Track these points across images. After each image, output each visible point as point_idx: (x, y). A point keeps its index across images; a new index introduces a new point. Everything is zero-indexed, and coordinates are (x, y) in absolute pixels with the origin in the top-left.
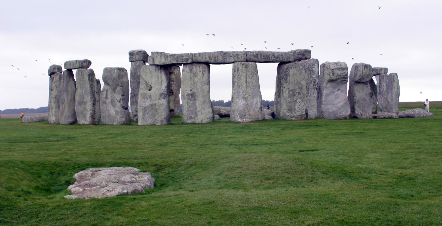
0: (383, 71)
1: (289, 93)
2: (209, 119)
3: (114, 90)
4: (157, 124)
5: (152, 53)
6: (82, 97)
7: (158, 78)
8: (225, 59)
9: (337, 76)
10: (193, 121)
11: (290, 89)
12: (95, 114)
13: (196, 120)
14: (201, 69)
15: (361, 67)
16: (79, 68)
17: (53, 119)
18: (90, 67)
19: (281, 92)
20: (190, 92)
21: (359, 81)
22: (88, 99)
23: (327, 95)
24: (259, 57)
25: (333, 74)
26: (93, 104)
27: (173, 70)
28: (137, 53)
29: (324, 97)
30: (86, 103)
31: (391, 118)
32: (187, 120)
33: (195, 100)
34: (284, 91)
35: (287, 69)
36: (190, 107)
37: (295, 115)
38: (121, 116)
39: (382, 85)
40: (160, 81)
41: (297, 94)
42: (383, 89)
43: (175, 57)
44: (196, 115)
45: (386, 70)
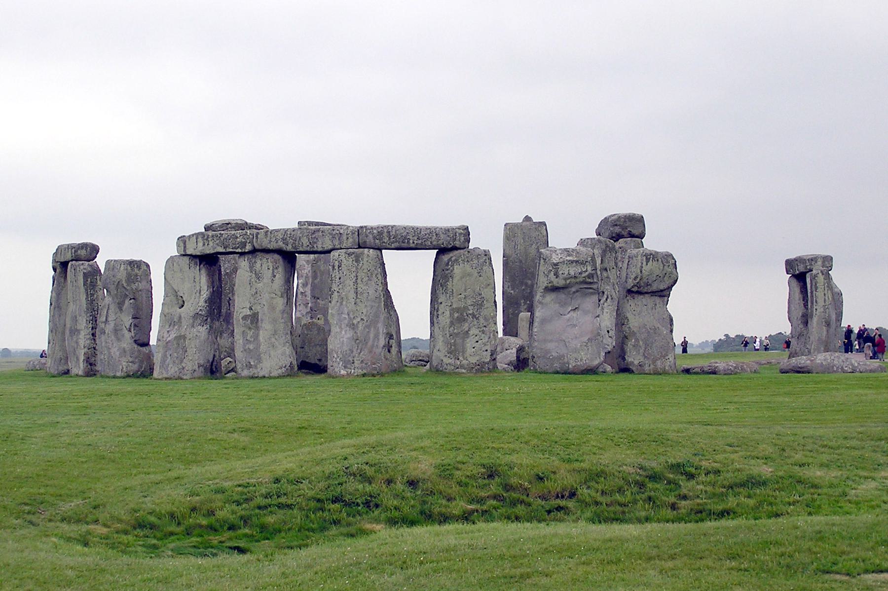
0: (820, 263)
3: (120, 306)
6: (75, 319)
9: (565, 279)
10: (253, 371)
11: (454, 306)
21: (635, 289)
26: (93, 335)
28: (219, 226)
30: (78, 331)
33: (257, 328)
34: (440, 313)
35: (447, 264)
36: (249, 342)
37: (465, 362)
38: (131, 360)
40: (198, 288)
44: (259, 360)
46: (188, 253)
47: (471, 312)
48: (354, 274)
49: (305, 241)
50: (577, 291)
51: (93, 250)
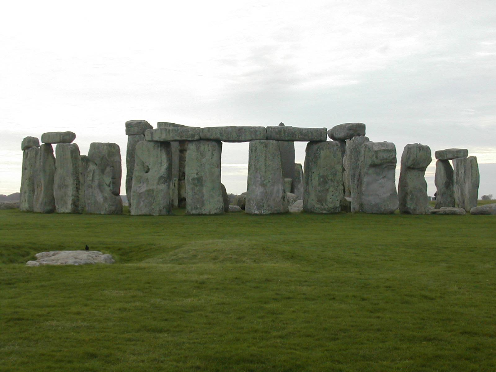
0: (462, 154)
1: (319, 179)
2: (218, 211)
3: (103, 171)
4: (154, 215)
5: (159, 124)
7: (157, 157)
8: (240, 136)
9: (381, 160)
10: (198, 211)
11: (321, 174)
12: (78, 200)
13: (203, 210)
14: (211, 148)
15: (415, 148)
16: (60, 142)
17: (25, 206)
18: (74, 142)
19: (310, 178)
20: (196, 176)
21: (412, 167)
22: (70, 181)
23: (368, 184)
24: (283, 135)
25: (377, 157)
26: (77, 188)
27: (186, 146)
29: (364, 185)
30: (66, 186)
31: (454, 214)
32: (192, 210)
33: (202, 185)
34: (313, 178)
35: (317, 150)
36: (196, 194)
37: (326, 207)
38: (111, 203)
39: (460, 173)
40: (159, 161)
41: (330, 182)
42: (461, 177)
43: (179, 132)
44: (203, 205)
45: (466, 152)
47: (330, 178)
50: (386, 167)
51: (72, 136)
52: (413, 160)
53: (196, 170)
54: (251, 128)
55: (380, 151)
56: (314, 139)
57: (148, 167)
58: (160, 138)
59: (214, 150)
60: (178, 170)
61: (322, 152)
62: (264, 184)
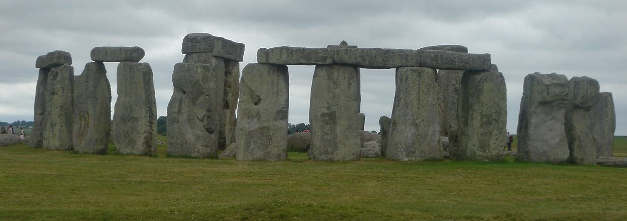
1: (481, 119)
3: (194, 101)
8: (387, 61)
10: (330, 156)
11: (484, 113)
16: (125, 61)
19: (470, 118)
20: (326, 111)
21: (580, 105)
24: (440, 61)
25: (548, 93)
26: (150, 122)
27: (231, 68)
28: (202, 39)
29: (532, 128)
30: (136, 119)
38: (205, 144)
44: (336, 148)
46: (271, 62)
47: (494, 118)
48: (417, 86)
49: (380, 59)
52: (583, 97)
53: (327, 103)
54: (401, 51)
55: (552, 84)
56: (476, 68)
57: (258, 98)
58: (278, 60)
59: (352, 78)
60: (223, 98)
61: (485, 84)
62: (416, 124)
